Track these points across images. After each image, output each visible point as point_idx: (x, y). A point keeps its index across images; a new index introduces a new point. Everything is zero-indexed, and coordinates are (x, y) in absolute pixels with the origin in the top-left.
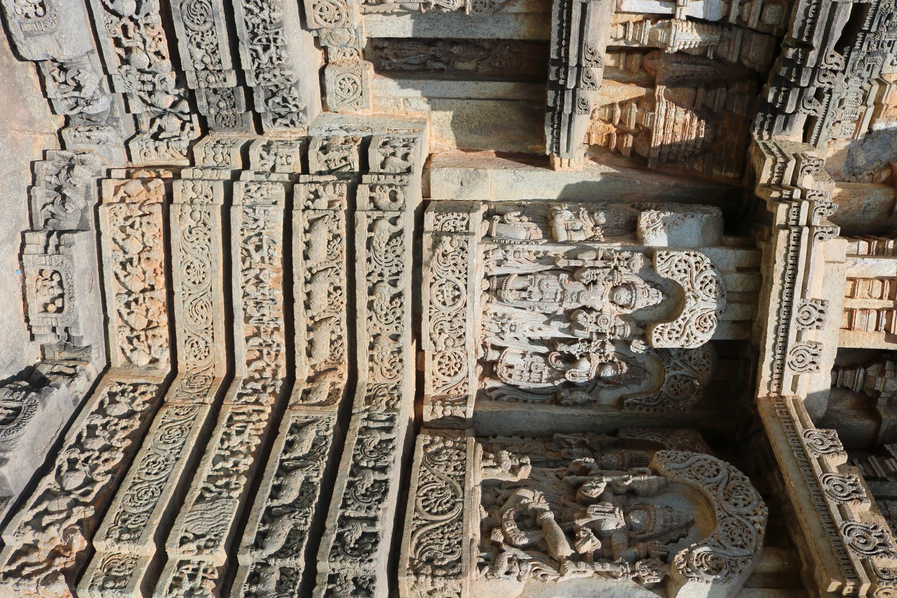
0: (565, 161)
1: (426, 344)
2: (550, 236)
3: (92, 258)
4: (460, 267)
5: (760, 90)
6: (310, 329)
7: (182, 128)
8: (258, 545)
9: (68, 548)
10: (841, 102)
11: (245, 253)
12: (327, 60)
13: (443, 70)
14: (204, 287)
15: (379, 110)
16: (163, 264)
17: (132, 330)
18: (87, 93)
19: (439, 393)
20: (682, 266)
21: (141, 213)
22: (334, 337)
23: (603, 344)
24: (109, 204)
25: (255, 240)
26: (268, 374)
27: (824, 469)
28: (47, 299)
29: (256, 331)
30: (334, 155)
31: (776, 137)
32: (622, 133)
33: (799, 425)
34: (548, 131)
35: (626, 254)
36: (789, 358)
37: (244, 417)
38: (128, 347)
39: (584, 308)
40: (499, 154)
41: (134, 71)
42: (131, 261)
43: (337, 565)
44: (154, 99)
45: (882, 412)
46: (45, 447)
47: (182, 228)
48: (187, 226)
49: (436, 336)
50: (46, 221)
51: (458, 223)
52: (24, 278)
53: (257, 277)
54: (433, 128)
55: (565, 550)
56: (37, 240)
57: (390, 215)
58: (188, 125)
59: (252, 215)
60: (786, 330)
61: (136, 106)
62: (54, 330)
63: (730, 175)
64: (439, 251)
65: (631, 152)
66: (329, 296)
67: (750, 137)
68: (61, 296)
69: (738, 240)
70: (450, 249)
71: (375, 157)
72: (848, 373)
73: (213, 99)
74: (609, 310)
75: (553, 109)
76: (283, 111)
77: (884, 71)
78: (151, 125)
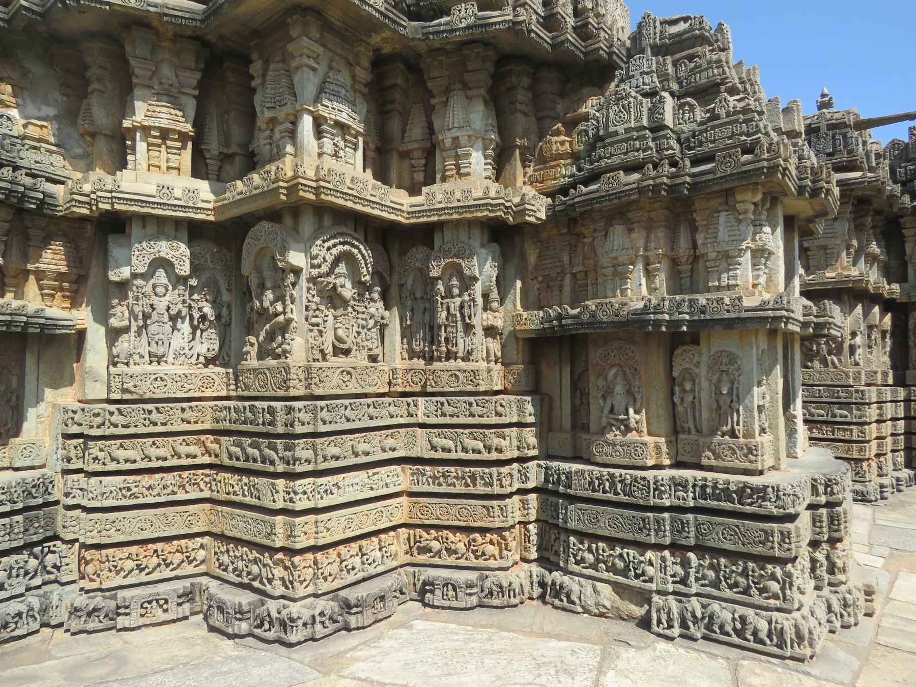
0: (80, 322)
1: (191, 394)
2: (126, 330)
4: (142, 378)
5: (29, 211)
6: (180, 457)
7: (54, 552)
8: (272, 463)
9: (282, 561)
10: (36, 162)
12: (7, 468)
13: (17, 397)
17: (183, 561)
18: (23, 608)
19: (225, 388)
20: (140, 258)
22: (184, 443)
23: (193, 300)
24: (101, 583)
25: (124, 491)
26: (207, 479)
27: (241, 193)
28: (160, 610)
30: (73, 453)
31: (61, 202)
32: (62, 289)
33: (225, 202)
34: (58, 332)
35: (134, 289)
36: (191, 204)
38: (195, 563)
39: (168, 311)
40: (78, 361)
41: (10, 581)
42: (138, 566)
43: (279, 424)
45: (231, 151)
46: (241, 591)
49: (186, 390)
50: (111, 619)
51: (117, 380)
52: (146, 626)
53: (148, 489)
54: (59, 400)
55: (281, 318)
56: (122, 622)
57: (108, 416)
59: (107, 494)
60: (175, 206)
61: (37, 581)
62: (180, 604)
63: (89, 227)
64: (133, 389)
65: (75, 285)
67: (61, 216)
68: (157, 601)
69: (127, 226)
70: (132, 383)
71: (75, 429)
72: (209, 168)
73: (32, 531)
74: (167, 298)
75: (42, 329)
76: (42, 490)
77: (16, 134)
78: (52, 573)
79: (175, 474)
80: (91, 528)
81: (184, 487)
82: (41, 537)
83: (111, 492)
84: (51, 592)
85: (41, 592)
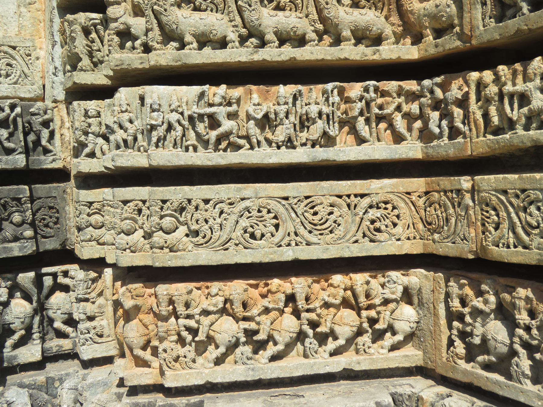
3: (249, 397)
11: (224, 145)
14: (282, 210)
15: (38, 31)
16: (252, 282)
17: (360, 332)
21: (173, 319)
24: (162, 373)
26: (415, 108)
29: (346, 129)
37: (493, 110)
38: (389, 340)
42: (250, 333)
44: (16, 324)
47: (190, 246)
48: (185, 239)
58: (61, 280)
59: (161, 131)
66: (283, 9)
79: (330, 86)
80: (127, 225)
81: (349, 124)
82: (29, 248)
83: (170, 128)
84: (61, 380)
85: (39, 377)
